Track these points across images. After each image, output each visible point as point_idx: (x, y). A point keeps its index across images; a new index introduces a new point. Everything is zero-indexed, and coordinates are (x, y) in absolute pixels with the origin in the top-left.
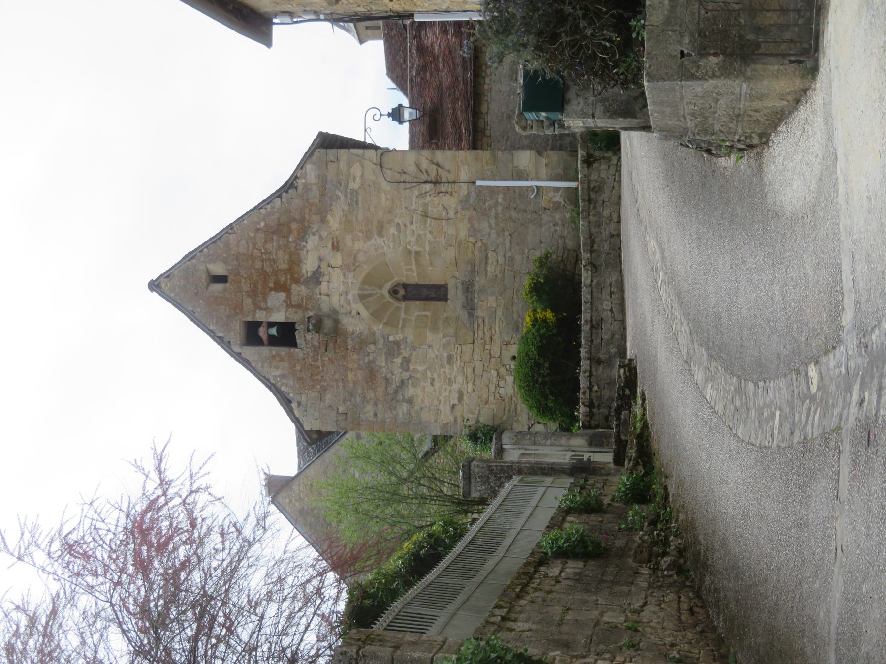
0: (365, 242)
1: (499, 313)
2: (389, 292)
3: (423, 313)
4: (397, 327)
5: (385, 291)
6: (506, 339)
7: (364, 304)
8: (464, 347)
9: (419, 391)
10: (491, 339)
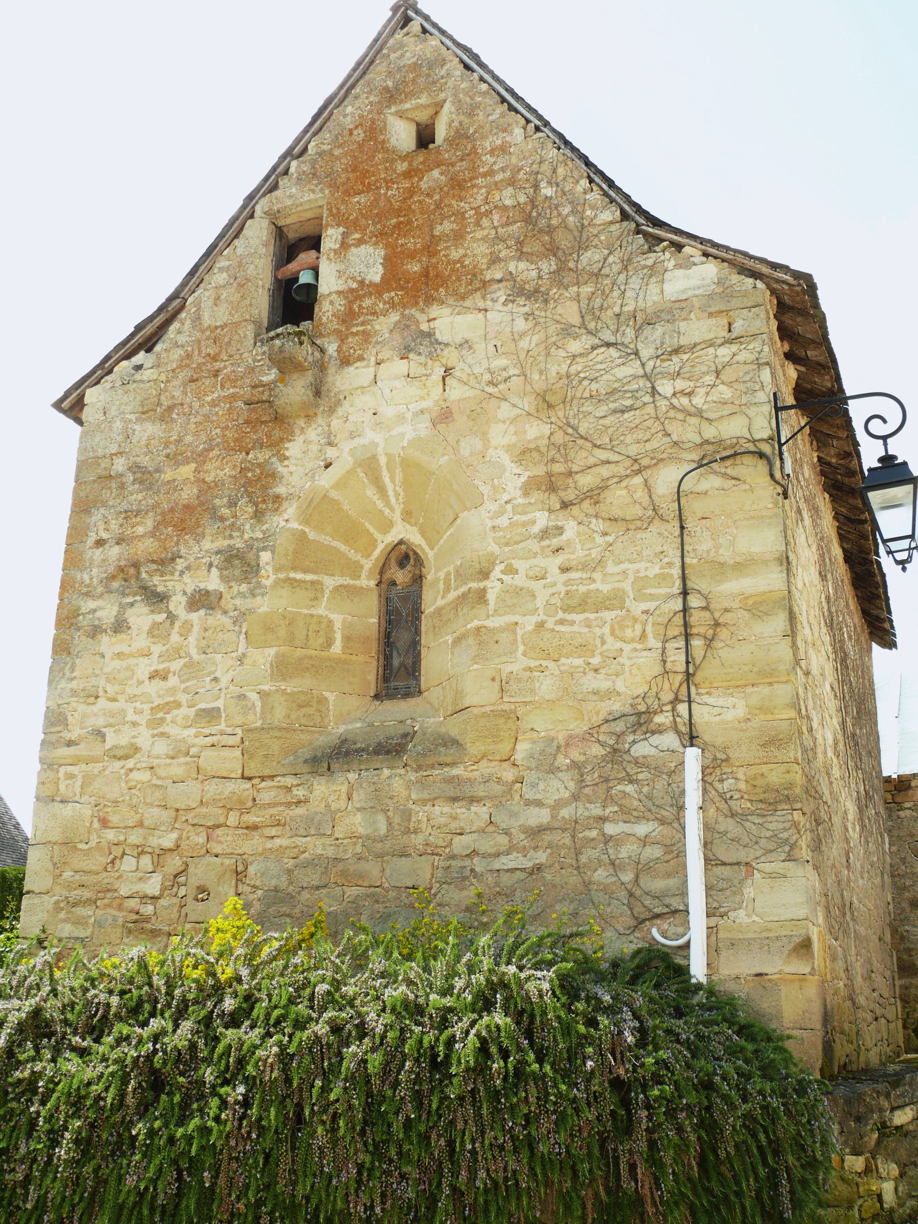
0: (509, 448)
1: (317, 847)
2: (401, 542)
3: (338, 636)
4: (294, 569)
5: (401, 531)
6: (251, 870)
7: (351, 473)
8: (238, 753)
9: (141, 641)
10: (254, 828)
